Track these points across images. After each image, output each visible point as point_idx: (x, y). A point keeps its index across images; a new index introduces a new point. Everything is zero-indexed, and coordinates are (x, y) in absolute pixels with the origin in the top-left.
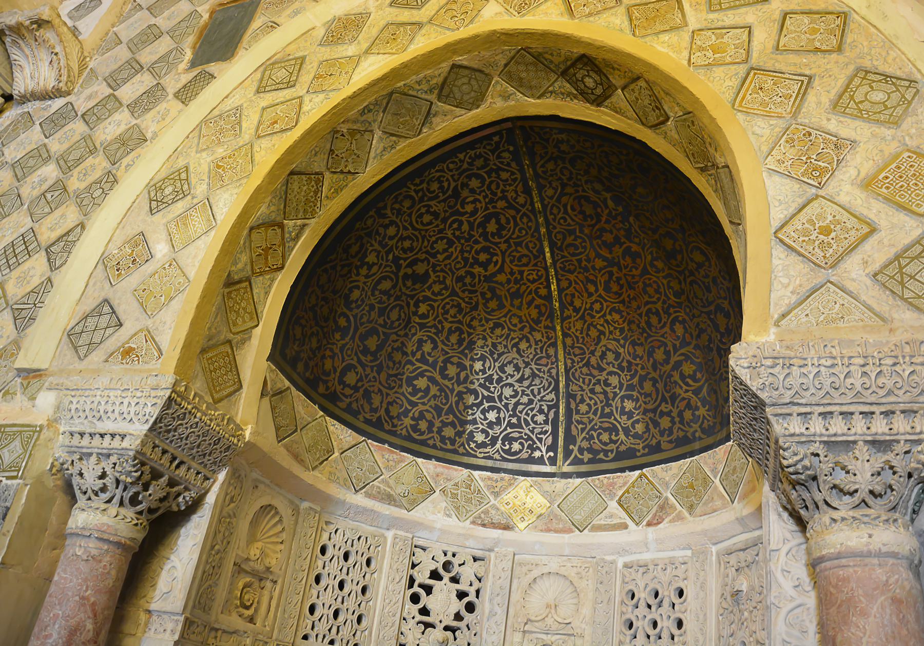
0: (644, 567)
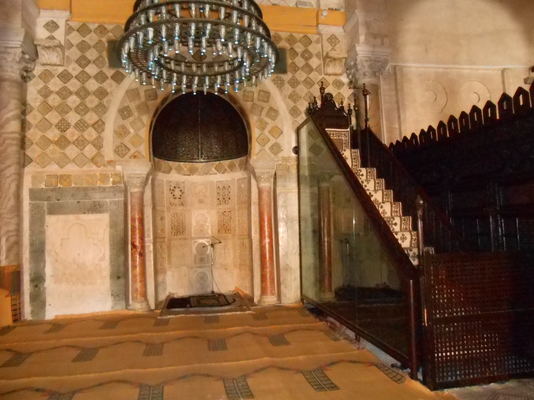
0: (221, 182)
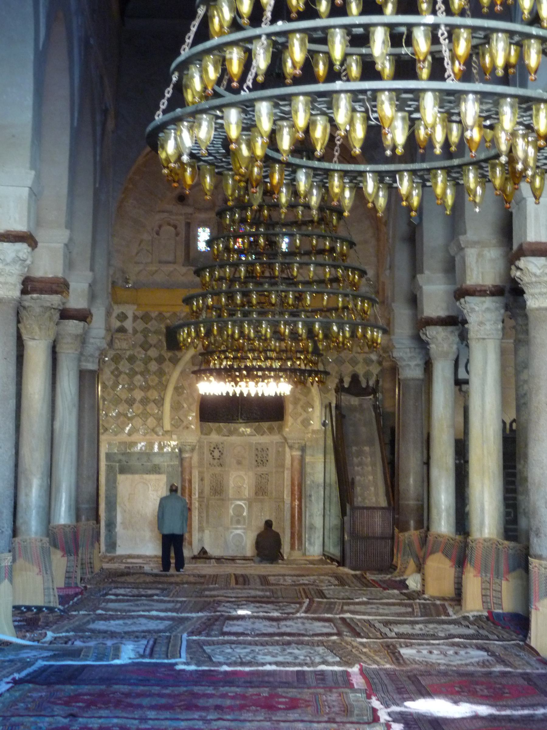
0: (260, 444)
